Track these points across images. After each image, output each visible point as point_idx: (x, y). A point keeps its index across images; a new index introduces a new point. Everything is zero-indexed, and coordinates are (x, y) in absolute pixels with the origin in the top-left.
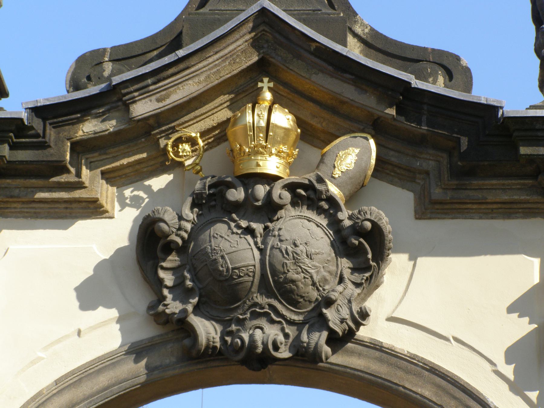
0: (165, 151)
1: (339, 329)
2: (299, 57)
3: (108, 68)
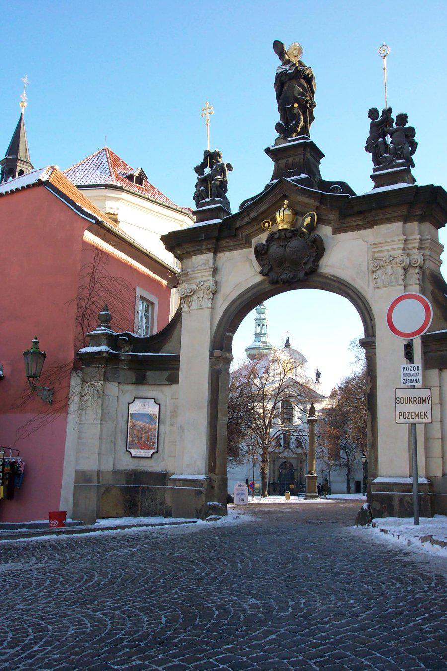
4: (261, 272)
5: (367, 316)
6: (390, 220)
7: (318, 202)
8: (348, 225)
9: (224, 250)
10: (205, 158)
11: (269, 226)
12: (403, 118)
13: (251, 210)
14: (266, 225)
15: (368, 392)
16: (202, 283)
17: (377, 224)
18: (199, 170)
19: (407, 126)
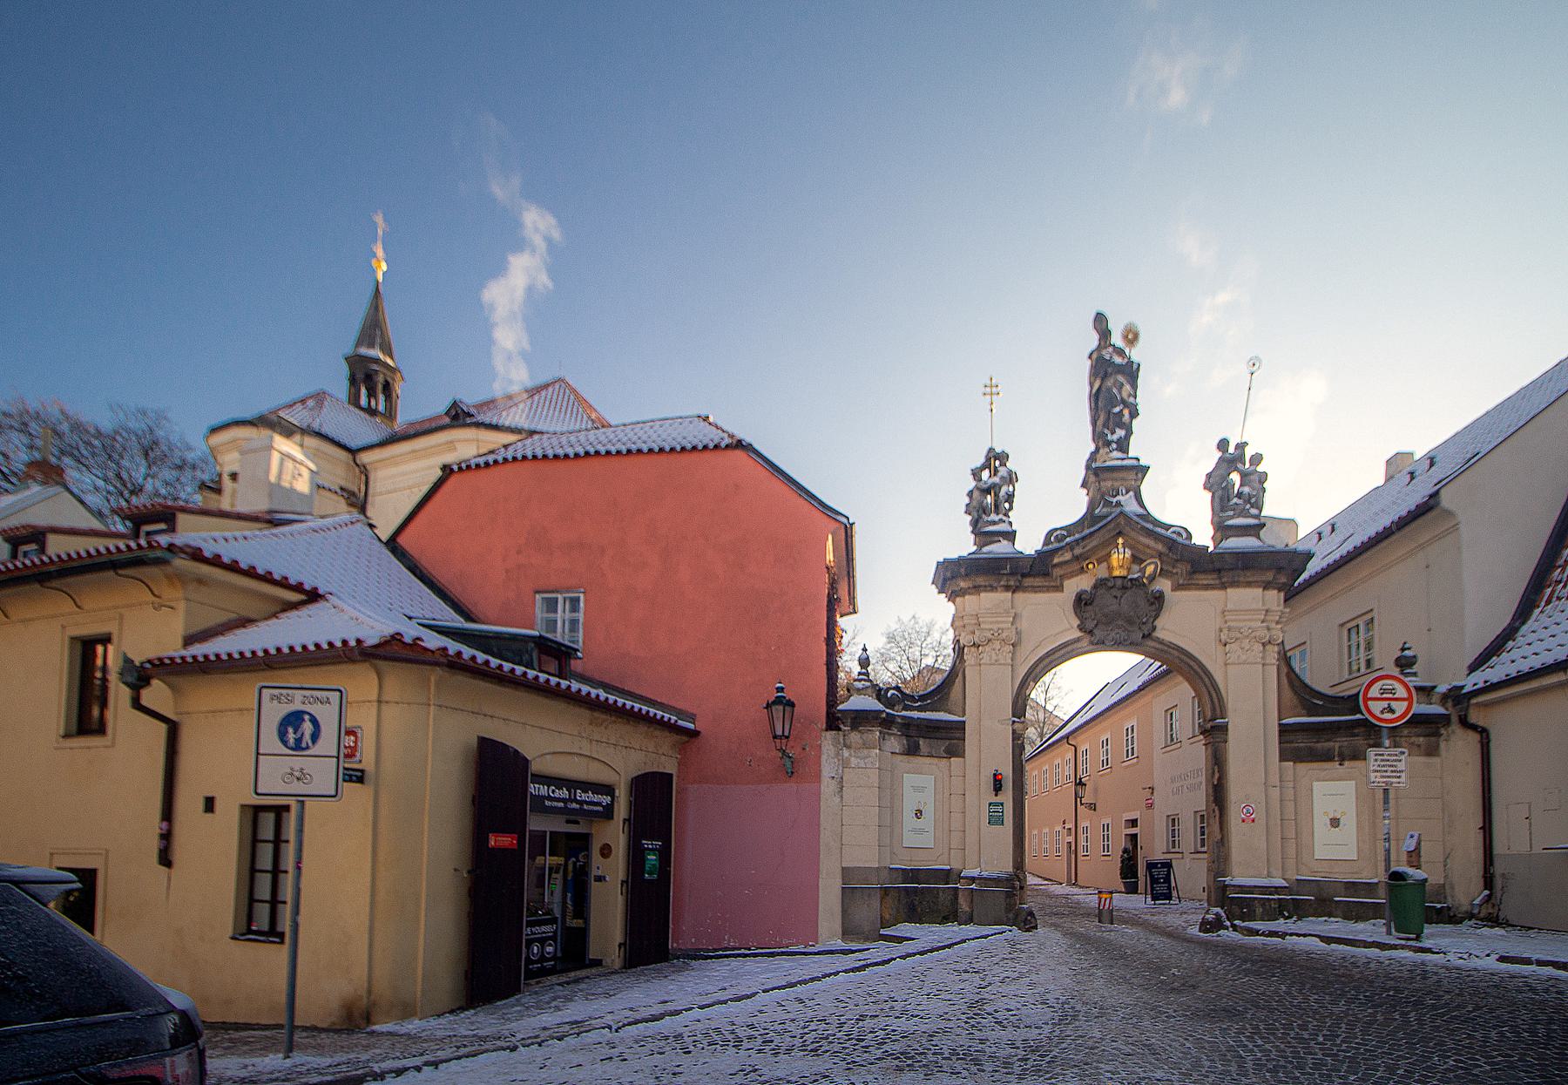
0: (1083, 568)
1: (1146, 633)
4: (1081, 628)
6: (1249, 584)
13: (1078, 544)
14: (1091, 566)
16: (1000, 631)
18: (976, 474)
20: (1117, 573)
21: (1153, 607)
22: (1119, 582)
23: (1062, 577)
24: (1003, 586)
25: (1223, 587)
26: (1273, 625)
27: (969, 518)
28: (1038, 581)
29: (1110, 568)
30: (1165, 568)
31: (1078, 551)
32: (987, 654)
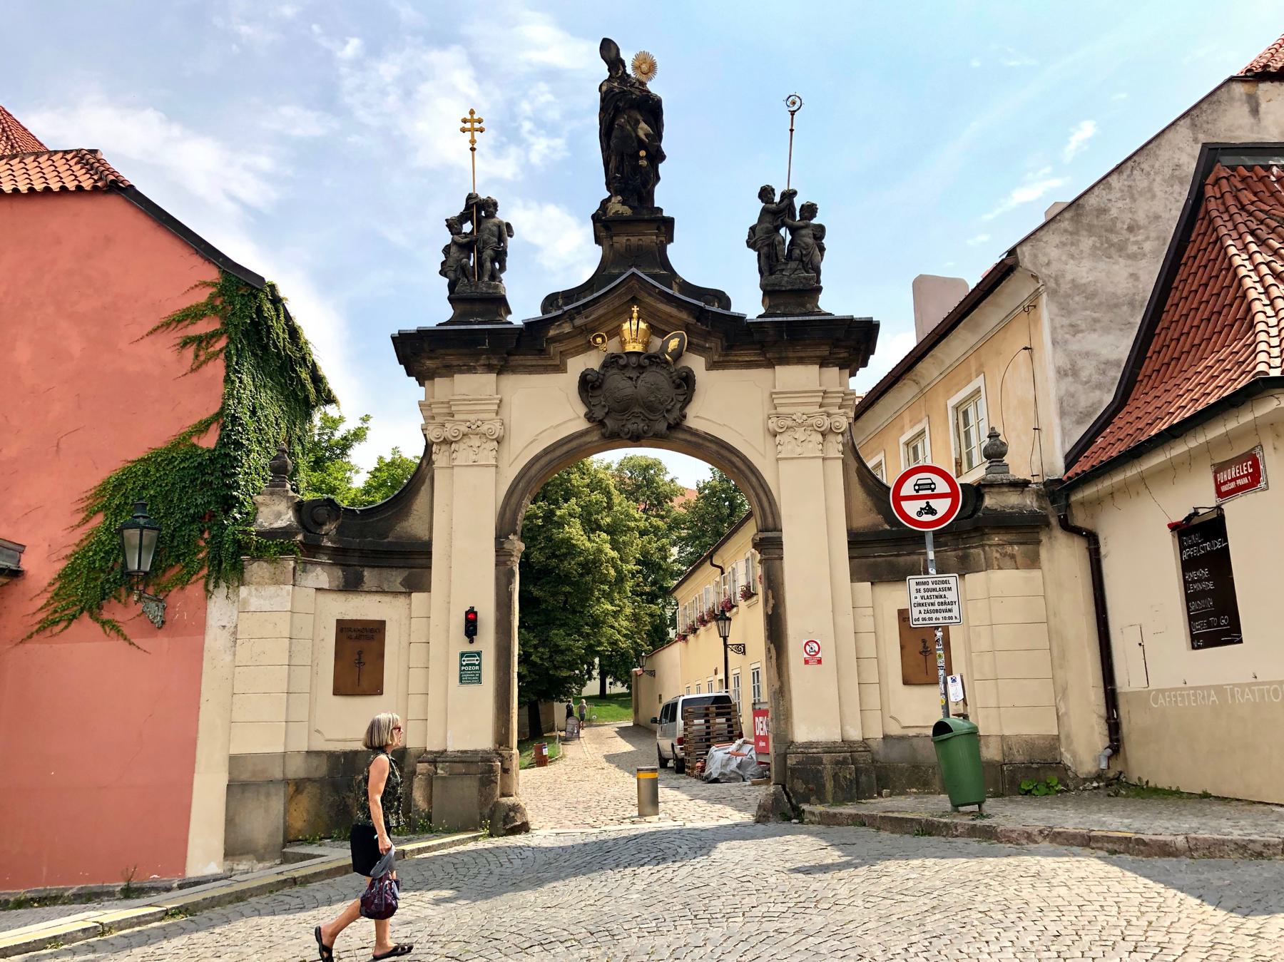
1: (671, 422)
2: (650, 295)
3: (561, 302)
4: (589, 417)
5: (764, 499)
6: (801, 361)
7: (694, 318)
8: (736, 358)
9: (514, 370)
10: (468, 207)
11: (603, 341)
12: (810, 210)
14: (599, 340)
15: (770, 613)
16: (479, 423)
17: (780, 364)
19: (815, 221)
20: (631, 347)
21: (679, 391)
22: (634, 359)
23: (565, 355)
24: (484, 365)
25: (770, 364)
26: (835, 410)
27: (447, 281)
28: (531, 360)
29: (623, 343)
30: (695, 341)
31: (579, 321)
32: (463, 454)
